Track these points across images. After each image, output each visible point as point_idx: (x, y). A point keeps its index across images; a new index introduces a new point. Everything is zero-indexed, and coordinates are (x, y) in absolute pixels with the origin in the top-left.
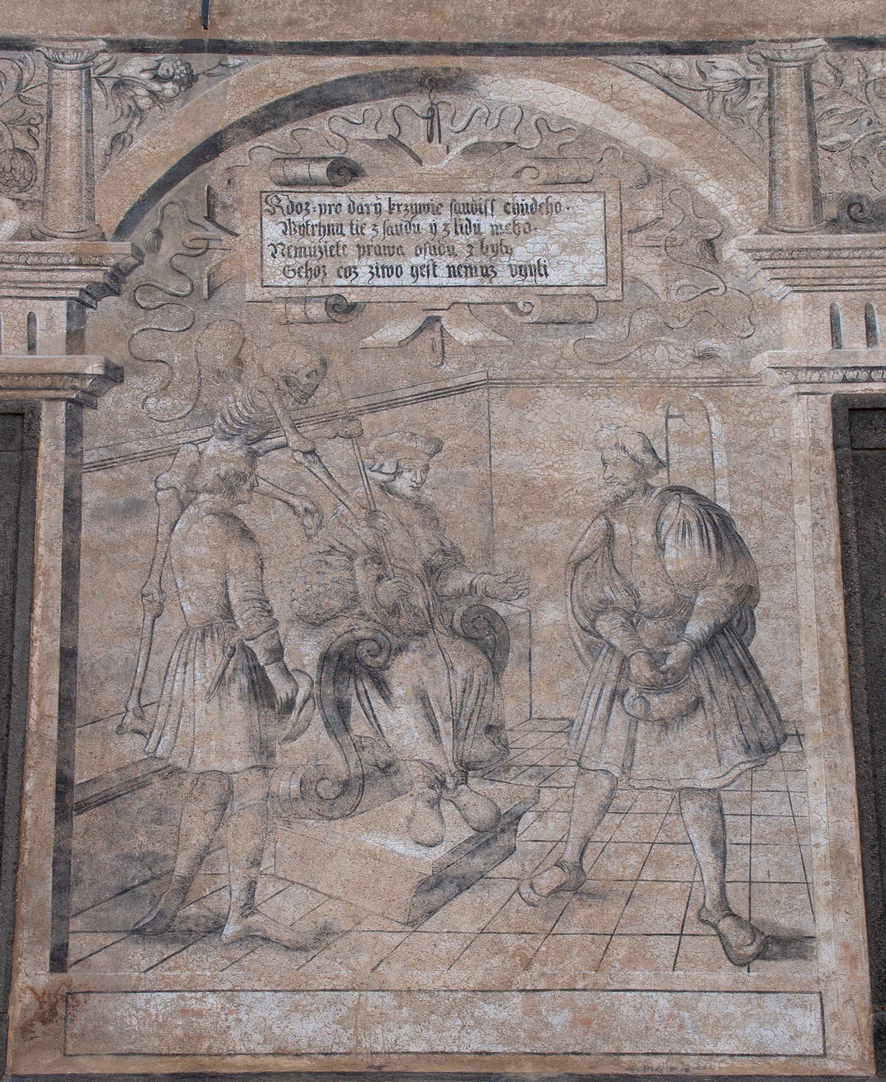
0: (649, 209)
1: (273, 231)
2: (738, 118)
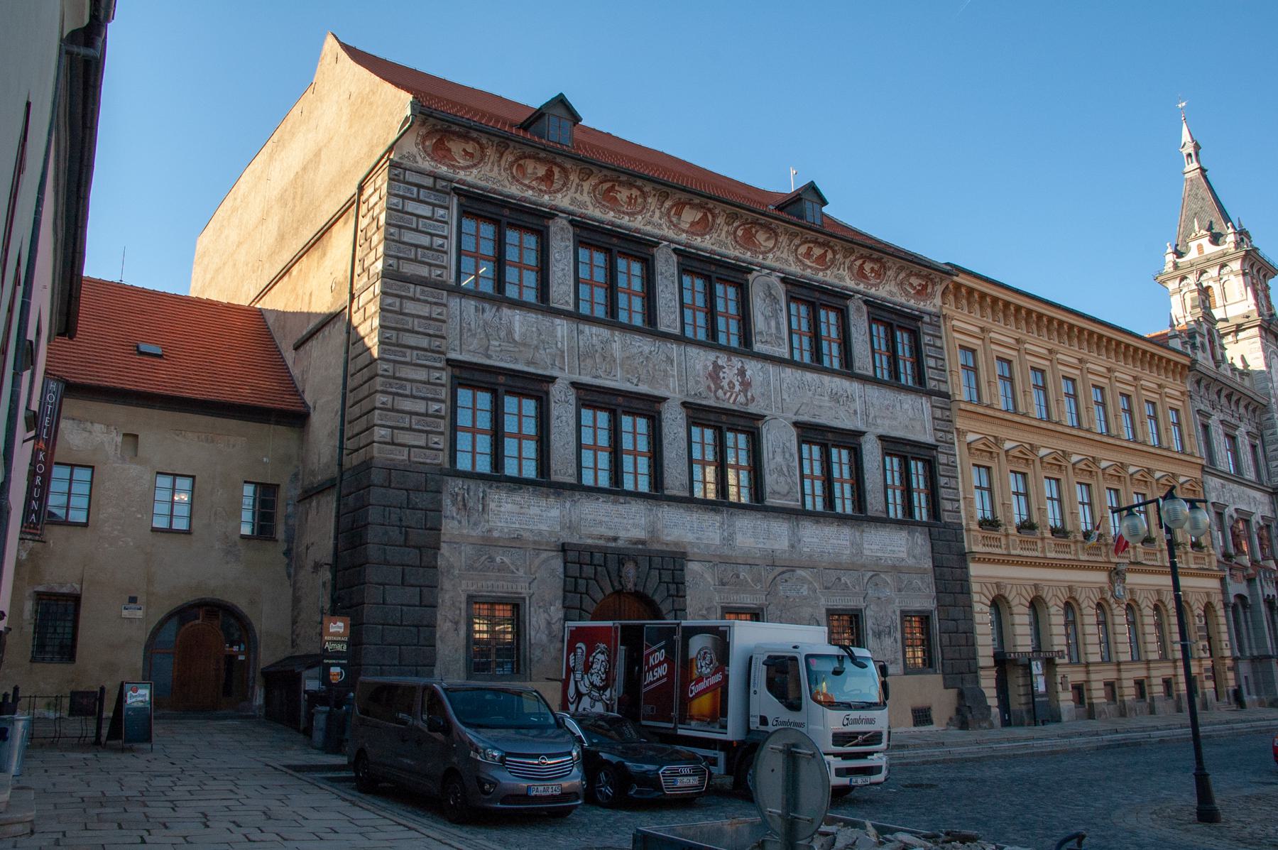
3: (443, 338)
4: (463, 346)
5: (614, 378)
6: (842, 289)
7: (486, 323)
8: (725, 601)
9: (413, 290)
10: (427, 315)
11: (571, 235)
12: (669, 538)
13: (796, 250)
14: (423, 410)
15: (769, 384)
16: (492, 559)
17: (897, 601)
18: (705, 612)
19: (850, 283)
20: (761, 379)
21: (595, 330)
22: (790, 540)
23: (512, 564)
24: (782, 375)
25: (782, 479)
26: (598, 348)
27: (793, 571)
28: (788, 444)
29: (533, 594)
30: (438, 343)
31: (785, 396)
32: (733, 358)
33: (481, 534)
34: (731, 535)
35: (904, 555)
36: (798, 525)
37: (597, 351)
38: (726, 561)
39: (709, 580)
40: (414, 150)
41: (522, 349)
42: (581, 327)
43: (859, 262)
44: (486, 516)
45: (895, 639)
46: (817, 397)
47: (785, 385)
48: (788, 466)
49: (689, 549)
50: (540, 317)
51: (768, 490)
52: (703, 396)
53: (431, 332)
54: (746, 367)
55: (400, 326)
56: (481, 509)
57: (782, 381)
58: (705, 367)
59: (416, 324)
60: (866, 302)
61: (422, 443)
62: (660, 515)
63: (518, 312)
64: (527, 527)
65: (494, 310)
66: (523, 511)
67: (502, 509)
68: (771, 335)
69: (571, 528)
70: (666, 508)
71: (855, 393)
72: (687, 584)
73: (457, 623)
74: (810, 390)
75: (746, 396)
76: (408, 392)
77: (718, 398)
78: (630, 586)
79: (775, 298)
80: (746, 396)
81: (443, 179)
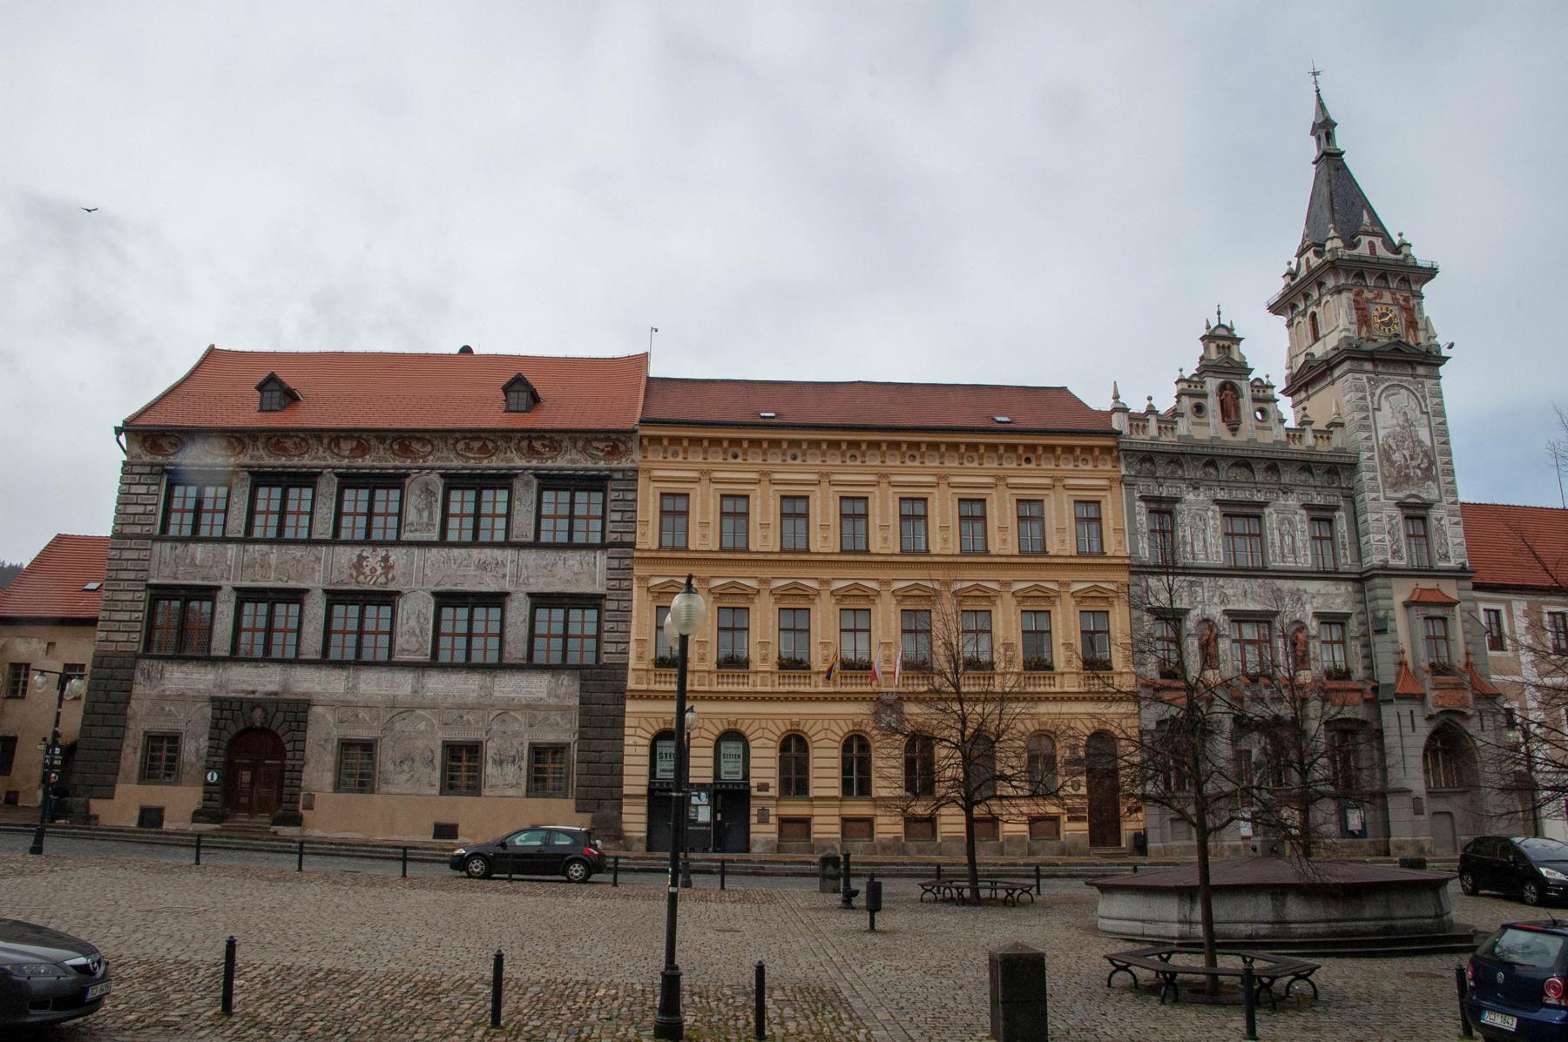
6: (508, 469)
7: (177, 556)
11: (249, 483)
13: (455, 448)
15: (412, 564)
16: (163, 709)
17: (526, 735)
19: (520, 462)
21: (257, 547)
22: (413, 687)
24: (428, 555)
25: (413, 639)
28: (424, 611)
31: (428, 571)
34: (355, 686)
35: (544, 695)
38: (347, 705)
40: (139, 451)
42: (247, 547)
45: (520, 767)
47: (429, 562)
49: (315, 697)
50: (216, 545)
51: (397, 648)
54: (390, 554)
58: (351, 560)
59: (129, 565)
60: (537, 476)
61: (125, 639)
62: (293, 673)
69: (220, 686)
70: (299, 669)
73: (135, 748)
75: (387, 577)
78: (258, 724)
79: (432, 492)
80: (387, 577)
81: (158, 465)
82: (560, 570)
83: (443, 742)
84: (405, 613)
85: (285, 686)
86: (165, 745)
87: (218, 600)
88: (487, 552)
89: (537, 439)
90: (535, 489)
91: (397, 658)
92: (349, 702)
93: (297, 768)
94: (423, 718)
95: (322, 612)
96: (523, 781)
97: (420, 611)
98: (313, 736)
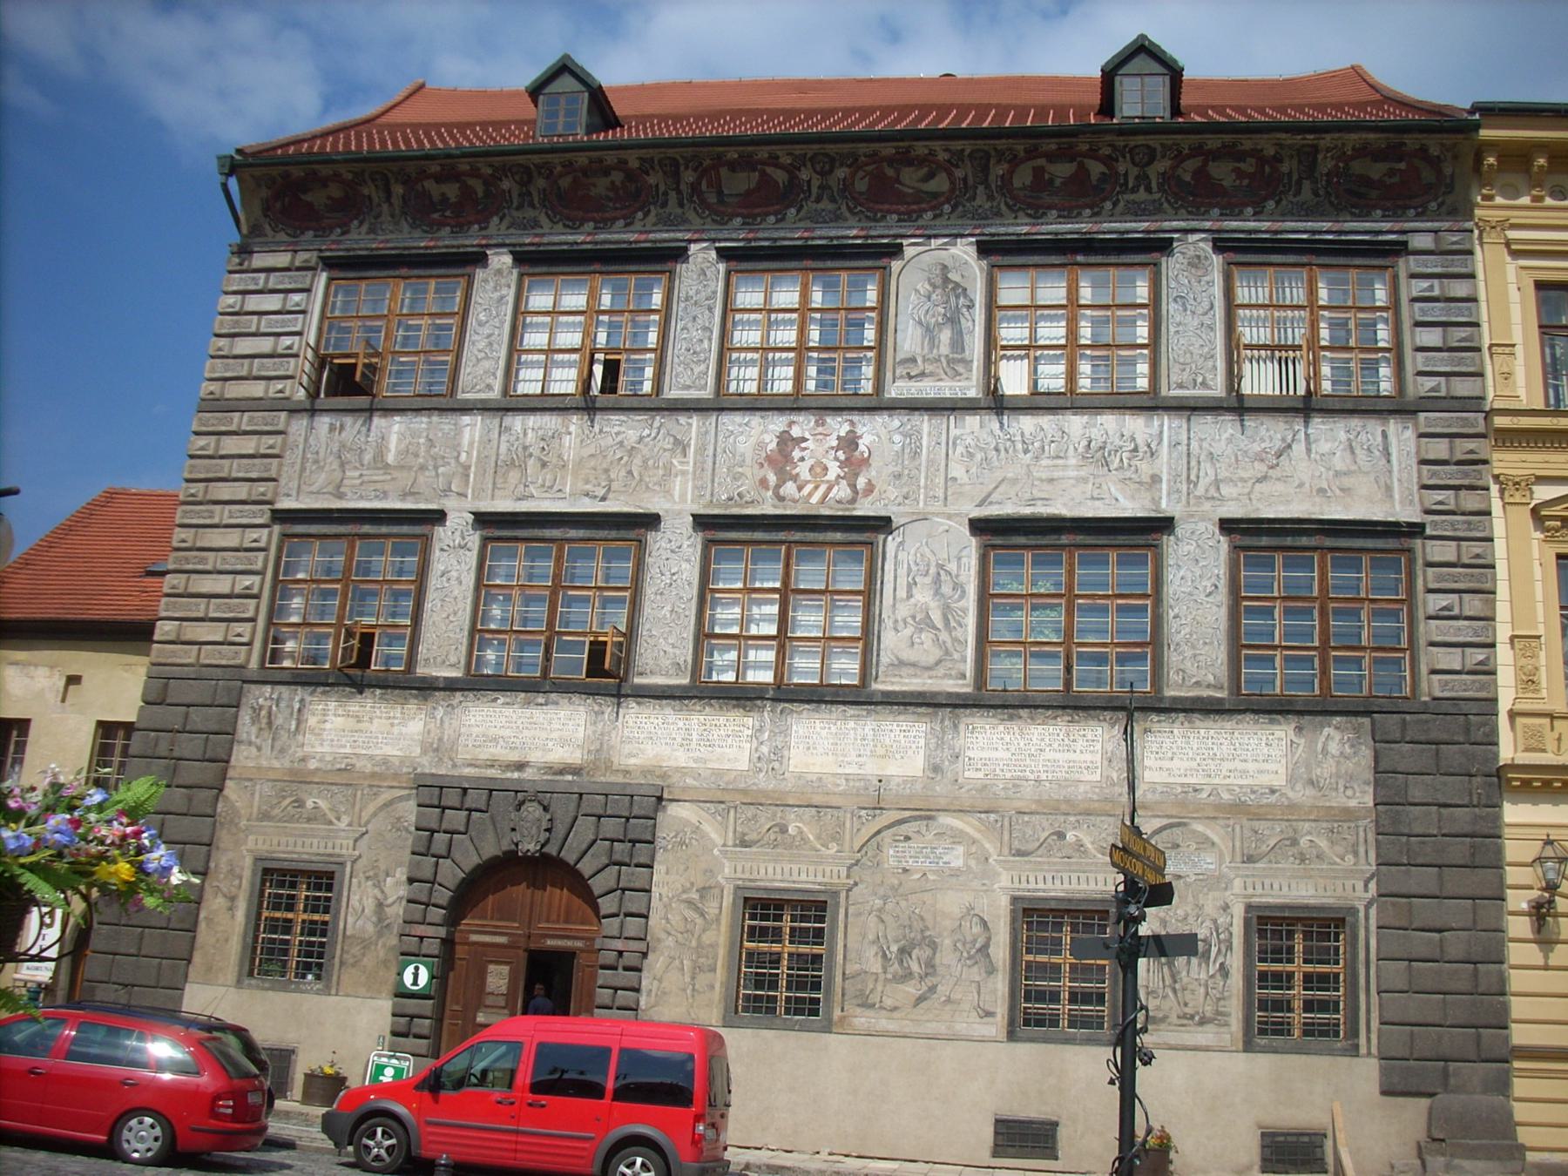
0: (974, 849)
1: (891, 852)
2: (995, 829)
3: (274, 480)
4: (304, 487)
5: (560, 495)
7: (343, 445)
8: (747, 876)
9: (238, 420)
10: (251, 452)
12: (632, 761)
14: (226, 590)
15: (916, 454)
16: (300, 803)
17: (1238, 884)
18: (695, 896)
20: (897, 447)
21: (533, 420)
22: (928, 757)
23: (331, 809)
24: (954, 432)
25: (926, 637)
26: (534, 450)
27: (930, 818)
28: (952, 567)
29: (360, 856)
30: (262, 489)
31: (957, 471)
32: (829, 420)
33: (287, 764)
34: (776, 751)
36: (956, 726)
37: (531, 455)
38: (756, 800)
39: (713, 835)
41: (396, 474)
43: (1192, 164)
44: (300, 738)
45: (1224, 971)
46: (1044, 462)
47: (960, 449)
48: (946, 610)
49: (675, 779)
50: (435, 419)
51: (885, 659)
52: (747, 498)
53: (254, 475)
54: (860, 430)
55: (210, 475)
56: (293, 727)
57: (951, 444)
58: (761, 445)
59: (236, 469)
61: (219, 638)
63: (397, 419)
64: (364, 752)
65: (360, 422)
66: (363, 726)
67: (328, 726)
68: (938, 360)
69: (436, 748)
71: (1160, 443)
72: (659, 842)
73: (233, 899)
74: (1026, 451)
75: (853, 486)
76: (209, 567)
77: (781, 499)
78: (530, 846)
79: (957, 285)
80: (853, 486)
82: (1299, 464)
83: (1015, 900)
84: (902, 572)
85: (600, 757)
86: (303, 893)
87: (436, 546)
88: (1108, 422)
89: (1215, 155)
90: (1217, 277)
91: (883, 684)
92: (764, 793)
93: (628, 959)
94: (957, 837)
95: (690, 571)
96: (1235, 1008)
97: (941, 567)
98: (667, 880)
